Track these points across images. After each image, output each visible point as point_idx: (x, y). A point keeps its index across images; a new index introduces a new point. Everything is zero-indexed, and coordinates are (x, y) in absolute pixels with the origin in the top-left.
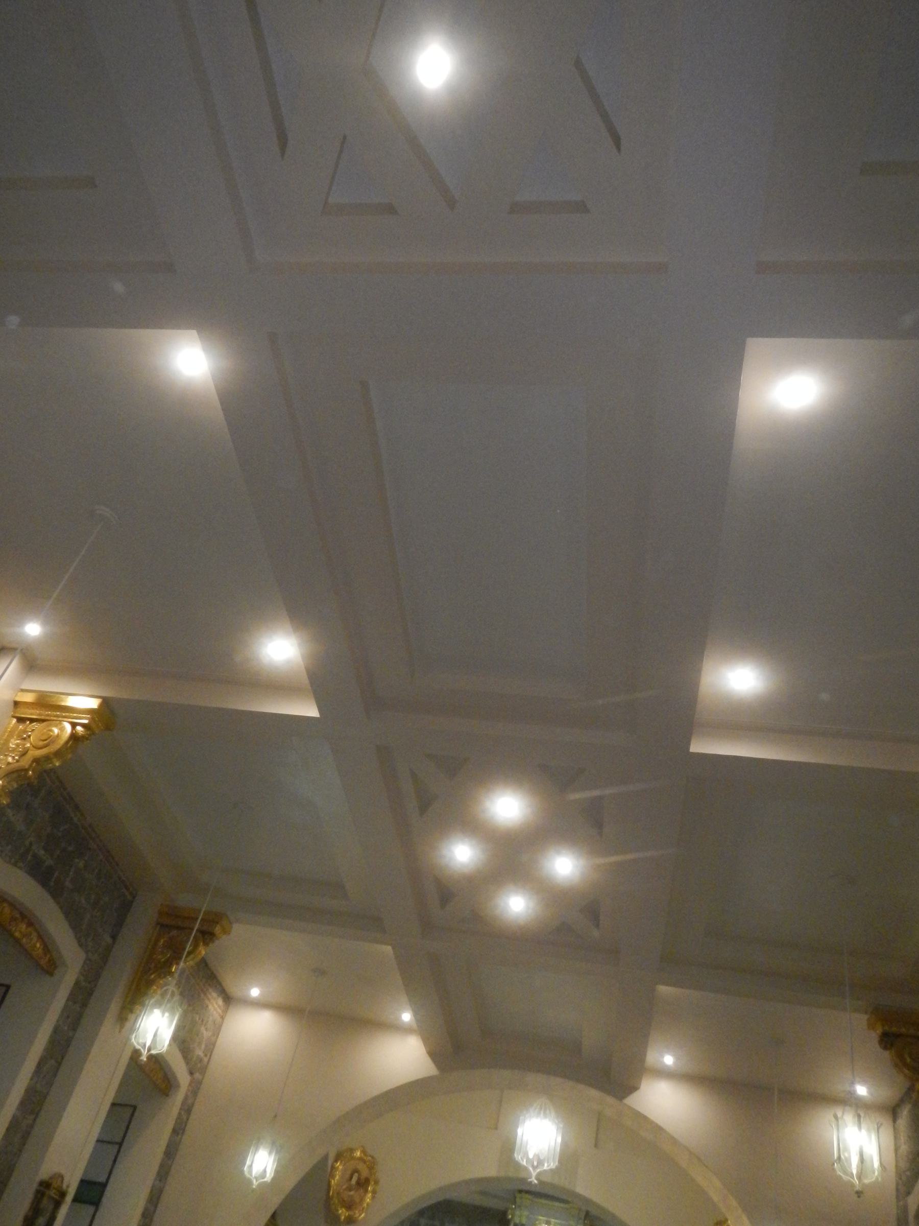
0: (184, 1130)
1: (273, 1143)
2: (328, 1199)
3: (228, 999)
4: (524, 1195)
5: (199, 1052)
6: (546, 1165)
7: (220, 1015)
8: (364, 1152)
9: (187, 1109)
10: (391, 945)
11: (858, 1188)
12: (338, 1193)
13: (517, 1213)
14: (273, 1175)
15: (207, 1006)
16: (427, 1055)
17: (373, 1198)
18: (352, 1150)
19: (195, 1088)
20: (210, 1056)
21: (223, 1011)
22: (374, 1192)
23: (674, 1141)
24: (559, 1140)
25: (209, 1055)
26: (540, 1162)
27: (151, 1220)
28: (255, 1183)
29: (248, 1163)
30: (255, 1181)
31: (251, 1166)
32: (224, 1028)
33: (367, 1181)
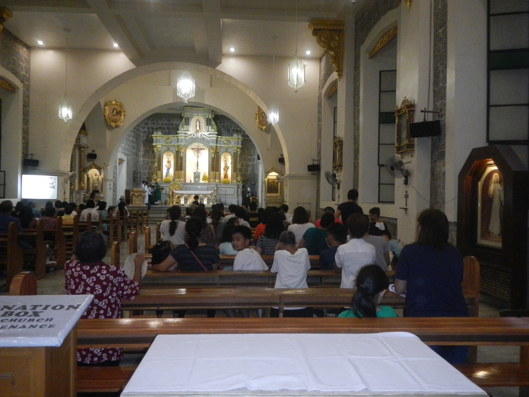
1: (68, 105)
2: (106, 120)
3: (30, 48)
6: (190, 96)
7: (27, 55)
8: (116, 101)
10: (96, 13)
11: (296, 90)
15: (19, 52)
16: (129, 60)
17: (125, 117)
18: (110, 102)
19: (27, 88)
21: (28, 53)
22: (124, 115)
23: (237, 81)
24: (194, 86)
25: (28, 73)
26: (188, 95)
27: (28, 139)
28: (65, 121)
29: (60, 113)
31: (61, 114)
32: (31, 61)
33: (120, 112)
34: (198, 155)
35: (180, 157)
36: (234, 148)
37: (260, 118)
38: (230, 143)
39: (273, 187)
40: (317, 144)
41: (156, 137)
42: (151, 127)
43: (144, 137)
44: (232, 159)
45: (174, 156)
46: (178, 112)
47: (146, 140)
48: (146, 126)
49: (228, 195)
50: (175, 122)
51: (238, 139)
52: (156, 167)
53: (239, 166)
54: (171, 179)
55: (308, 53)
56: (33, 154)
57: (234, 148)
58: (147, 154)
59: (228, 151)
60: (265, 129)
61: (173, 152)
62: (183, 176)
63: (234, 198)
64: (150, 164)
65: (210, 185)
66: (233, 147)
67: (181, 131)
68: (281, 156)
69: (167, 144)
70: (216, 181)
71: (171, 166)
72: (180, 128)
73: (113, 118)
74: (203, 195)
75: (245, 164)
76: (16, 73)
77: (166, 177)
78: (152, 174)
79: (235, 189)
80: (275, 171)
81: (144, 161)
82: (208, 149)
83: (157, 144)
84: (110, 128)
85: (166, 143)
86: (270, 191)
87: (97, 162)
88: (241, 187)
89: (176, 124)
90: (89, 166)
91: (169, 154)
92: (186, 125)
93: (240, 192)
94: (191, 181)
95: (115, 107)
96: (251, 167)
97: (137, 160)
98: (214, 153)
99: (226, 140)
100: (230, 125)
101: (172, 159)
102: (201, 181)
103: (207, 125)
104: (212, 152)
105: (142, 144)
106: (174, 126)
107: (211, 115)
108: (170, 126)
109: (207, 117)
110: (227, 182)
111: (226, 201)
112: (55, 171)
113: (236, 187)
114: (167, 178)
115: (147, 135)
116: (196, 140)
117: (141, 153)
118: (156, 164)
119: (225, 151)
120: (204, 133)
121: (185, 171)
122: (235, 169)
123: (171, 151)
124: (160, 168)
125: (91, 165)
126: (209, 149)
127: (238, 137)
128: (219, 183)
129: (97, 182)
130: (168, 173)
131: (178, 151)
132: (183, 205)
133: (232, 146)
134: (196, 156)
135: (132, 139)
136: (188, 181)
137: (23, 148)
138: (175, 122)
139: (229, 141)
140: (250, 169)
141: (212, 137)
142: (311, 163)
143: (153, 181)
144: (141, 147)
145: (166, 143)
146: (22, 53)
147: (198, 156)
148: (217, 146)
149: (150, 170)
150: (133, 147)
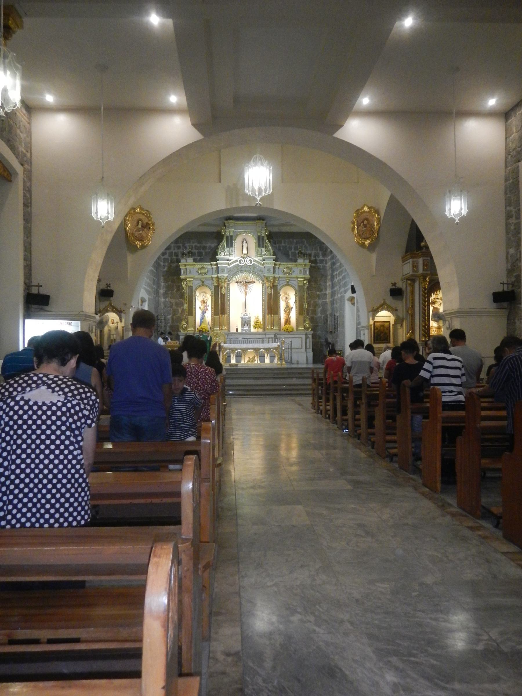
0: (31, 203)
1: (108, 195)
2: (127, 237)
4: (230, 221)
5: (22, 149)
7: (27, 122)
8: (141, 208)
9: (28, 191)
12: (132, 234)
13: (227, 231)
14: (114, 216)
15: (16, 113)
16: (192, 127)
17: (154, 233)
19: (29, 174)
20: (31, 150)
21: (28, 118)
25: (29, 151)
27: (31, 261)
30: (103, 223)
31: (97, 213)
32: (32, 130)
33: (148, 224)
34: (247, 290)
35: (222, 294)
36: (299, 279)
37: (360, 228)
38: (293, 272)
39: (382, 334)
40: (505, 257)
41: (185, 265)
42: (174, 252)
43: (164, 268)
44: (296, 296)
45: (212, 294)
46: (214, 229)
47: (167, 271)
48: (168, 252)
49: (294, 349)
50: (208, 245)
51: (305, 265)
52: (183, 310)
53: (306, 306)
54: (209, 327)
55: (492, 102)
56: (40, 284)
57: (299, 279)
58: (169, 292)
59: (290, 283)
60: (369, 244)
61: (210, 288)
62: (226, 323)
63: (302, 353)
64: (174, 307)
65: (266, 335)
66: (297, 278)
67: (221, 255)
68: (393, 286)
69: (200, 276)
70: (274, 328)
71: (208, 308)
72: (219, 251)
73: (137, 234)
74: (264, 349)
75: (312, 303)
76: (13, 148)
77: (200, 325)
78: (180, 320)
79: (302, 341)
80: (387, 310)
81: (164, 302)
82: (261, 281)
83: (188, 276)
84: (133, 249)
85: (199, 274)
86: (377, 340)
87: (115, 301)
88: (310, 336)
89: (210, 247)
90: (104, 309)
91: (204, 290)
92: (228, 246)
93: (310, 344)
94: (237, 329)
95: (140, 218)
96: (321, 308)
97: (158, 301)
98: (271, 287)
99: (287, 268)
100: (288, 246)
101: (207, 297)
102: (253, 330)
103: (259, 246)
104: (267, 285)
105: (162, 278)
106: (209, 250)
107: (263, 232)
108: (202, 250)
109: (259, 234)
110: (291, 330)
111: (291, 358)
112: (77, 313)
113: (303, 337)
114: (203, 326)
115: (169, 264)
116: (243, 269)
117: (162, 291)
118: (186, 306)
119: (286, 283)
120: (255, 259)
121: (229, 316)
122: (301, 311)
123: (207, 286)
124: (191, 311)
125: (106, 307)
126: (263, 281)
127: (304, 263)
128: (278, 331)
129: (115, 333)
130: (203, 318)
131: (218, 286)
132: (237, 365)
133: (295, 276)
134: (244, 293)
135: (153, 269)
136: (233, 330)
137: (25, 274)
138: (208, 245)
139: (292, 268)
140: (319, 310)
141: (267, 263)
142: (500, 289)
143: (182, 331)
144: (161, 282)
145: (199, 274)
146: (20, 116)
147: (246, 293)
148: (274, 278)
149: (174, 315)
150: (154, 280)
